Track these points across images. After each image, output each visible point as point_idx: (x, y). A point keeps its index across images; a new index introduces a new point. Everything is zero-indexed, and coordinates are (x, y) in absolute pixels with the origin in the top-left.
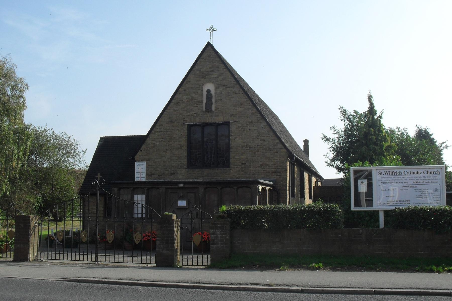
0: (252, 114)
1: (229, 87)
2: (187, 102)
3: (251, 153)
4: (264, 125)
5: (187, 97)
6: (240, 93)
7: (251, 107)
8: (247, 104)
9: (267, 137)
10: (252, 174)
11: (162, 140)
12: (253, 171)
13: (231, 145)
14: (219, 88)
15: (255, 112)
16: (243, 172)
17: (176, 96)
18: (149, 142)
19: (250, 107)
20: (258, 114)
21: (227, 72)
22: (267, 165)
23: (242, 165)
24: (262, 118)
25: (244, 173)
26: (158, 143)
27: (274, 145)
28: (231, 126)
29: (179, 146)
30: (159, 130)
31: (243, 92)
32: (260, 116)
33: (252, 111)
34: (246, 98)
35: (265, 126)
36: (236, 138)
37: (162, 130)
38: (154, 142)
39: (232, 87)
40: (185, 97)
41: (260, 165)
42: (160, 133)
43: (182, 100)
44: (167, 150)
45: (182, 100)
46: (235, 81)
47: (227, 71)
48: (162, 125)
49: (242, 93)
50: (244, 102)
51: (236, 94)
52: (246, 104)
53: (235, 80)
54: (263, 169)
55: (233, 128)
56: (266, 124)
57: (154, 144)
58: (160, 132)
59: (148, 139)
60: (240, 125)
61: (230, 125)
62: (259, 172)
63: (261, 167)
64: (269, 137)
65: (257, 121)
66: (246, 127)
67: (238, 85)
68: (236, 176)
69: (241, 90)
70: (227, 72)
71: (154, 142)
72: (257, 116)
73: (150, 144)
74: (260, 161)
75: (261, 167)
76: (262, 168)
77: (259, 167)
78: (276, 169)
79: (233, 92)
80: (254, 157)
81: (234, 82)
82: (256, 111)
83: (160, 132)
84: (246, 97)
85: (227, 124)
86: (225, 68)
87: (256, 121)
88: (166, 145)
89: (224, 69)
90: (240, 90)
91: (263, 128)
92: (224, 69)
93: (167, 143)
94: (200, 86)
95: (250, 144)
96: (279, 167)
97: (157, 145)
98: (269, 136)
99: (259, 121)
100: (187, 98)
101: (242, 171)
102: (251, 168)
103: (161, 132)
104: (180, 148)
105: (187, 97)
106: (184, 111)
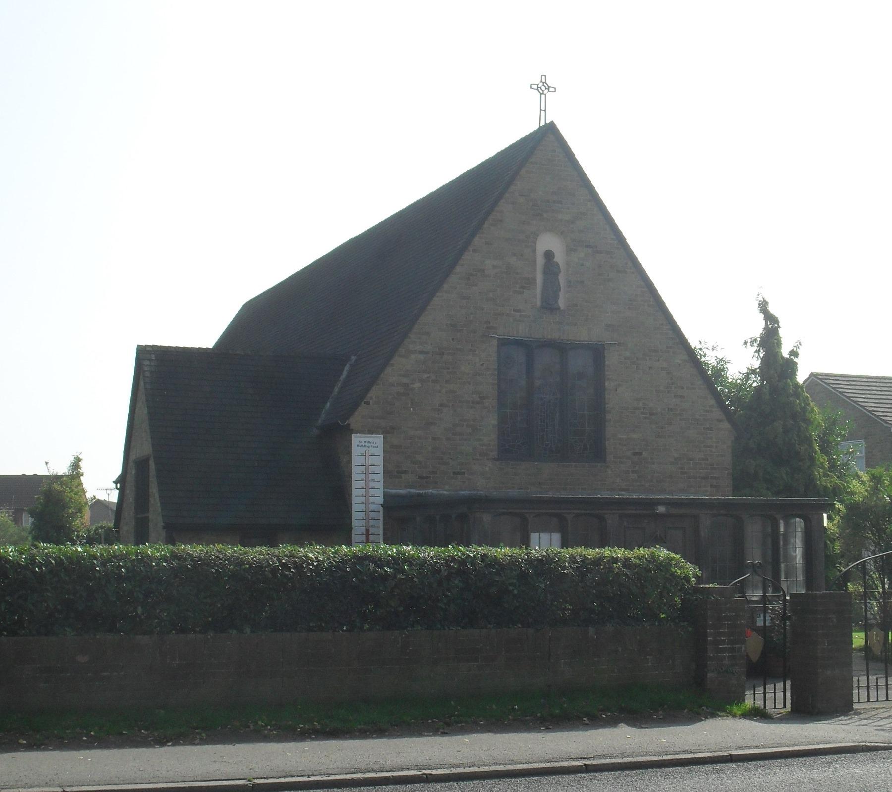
11: (428, 375)
13: (607, 404)
26: (417, 385)
38: (405, 380)
42: (422, 357)
43: (483, 271)
45: (483, 271)
46: (614, 237)
49: (633, 273)
51: (618, 271)
56: (686, 357)
58: (421, 352)
60: (628, 354)
65: (667, 347)
73: (393, 385)
83: (421, 352)
96: (715, 466)
100: (494, 267)
101: (633, 472)
103: (427, 353)
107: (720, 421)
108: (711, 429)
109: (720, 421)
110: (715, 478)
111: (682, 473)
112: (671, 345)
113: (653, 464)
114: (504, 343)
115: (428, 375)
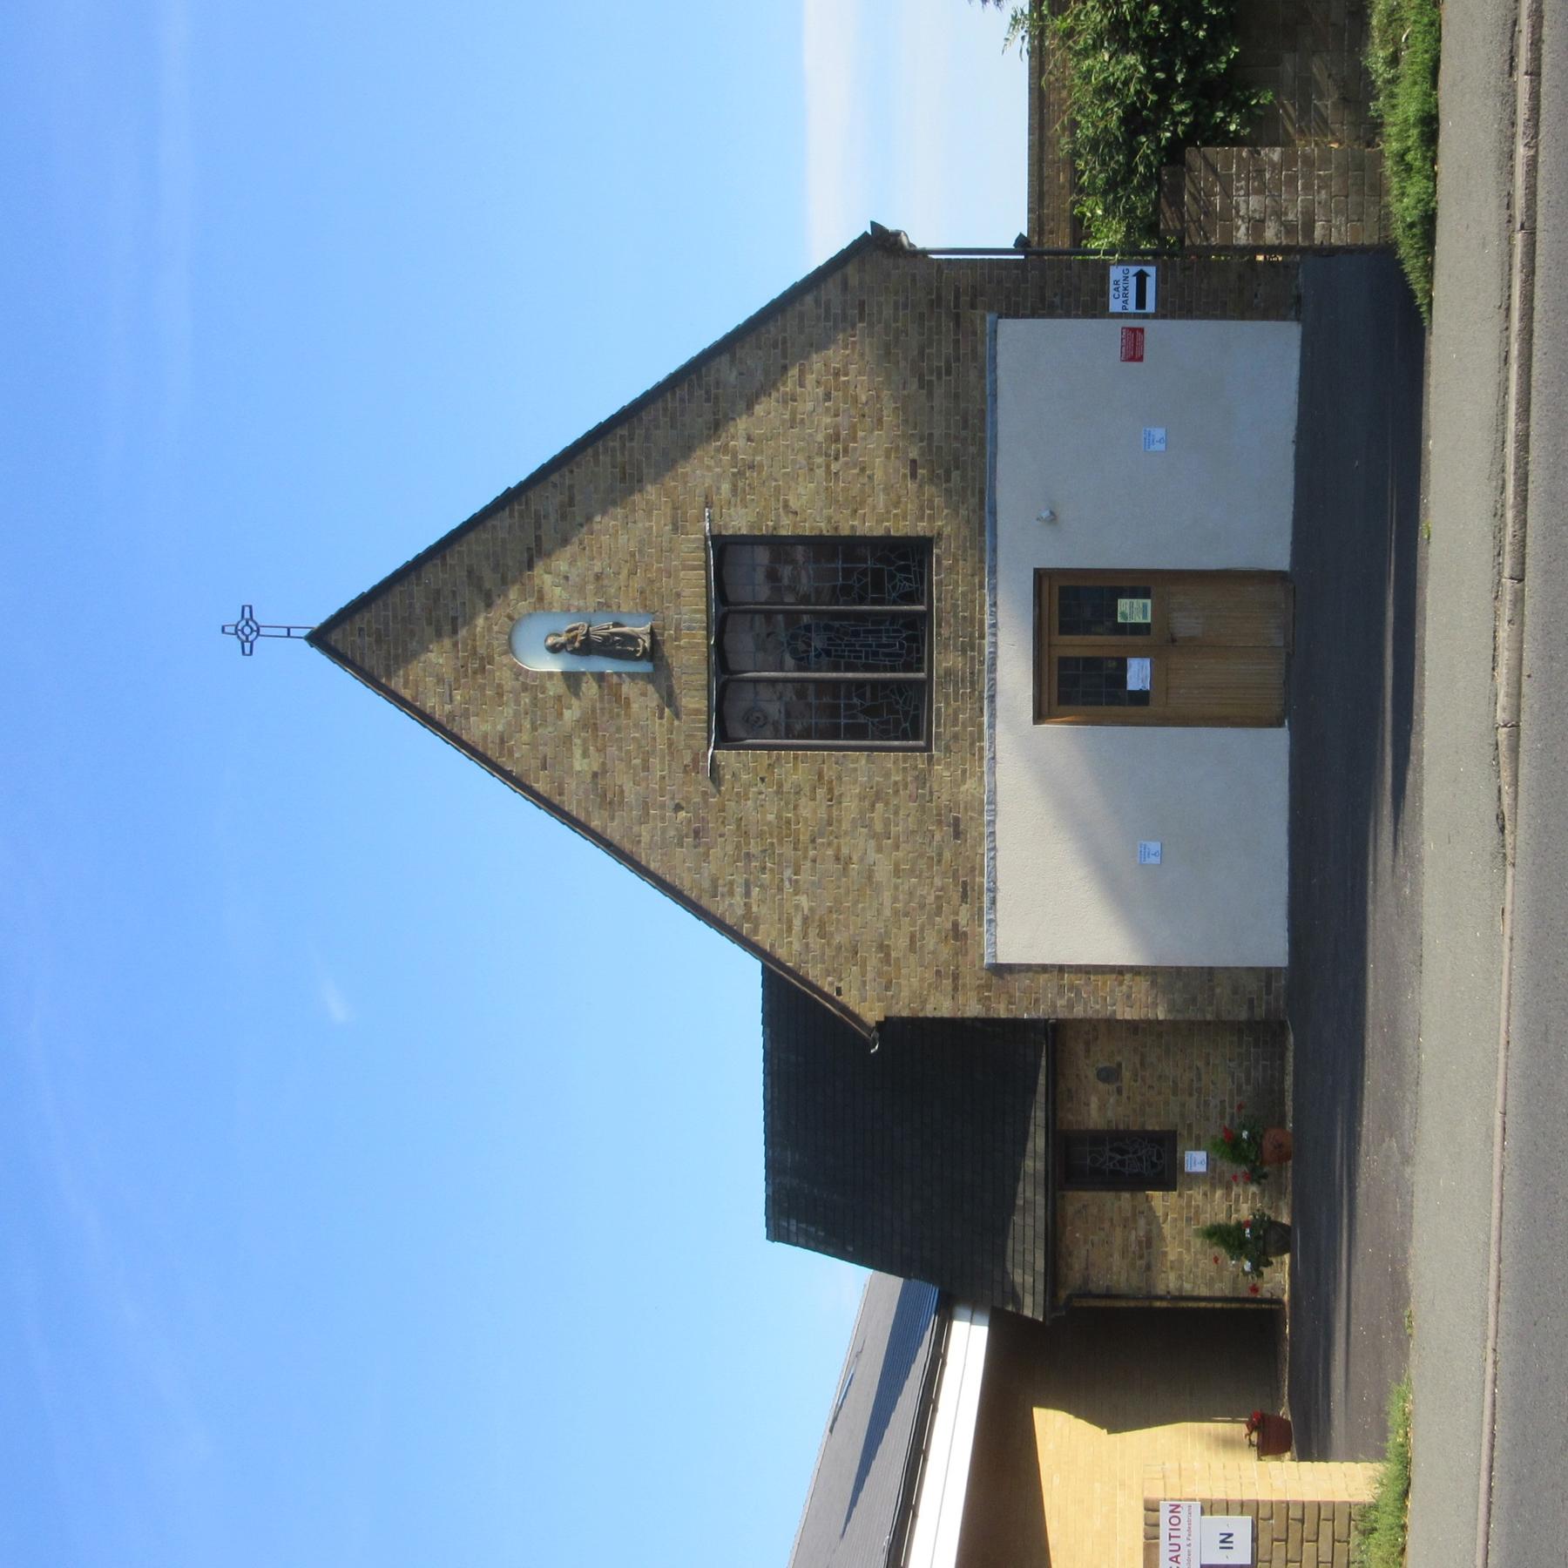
0: (671, 427)
1: (538, 539)
2: (601, 750)
3: (861, 434)
4: (730, 369)
5: (578, 752)
6: (567, 482)
7: (637, 431)
8: (623, 447)
9: (789, 351)
10: (965, 427)
11: (787, 883)
12: (948, 427)
13: (822, 531)
14: (540, 591)
15: (665, 410)
16: (955, 475)
17: (572, 808)
18: (796, 946)
19: (640, 432)
20: (674, 394)
21: (464, 548)
22: (921, 353)
23: (919, 477)
24: (694, 377)
25: (957, 468)
27: (827, 319)
28: (730, 532)
29: (821, 792)
30: (738, 899)
31: (565, 470)
32: (686, 386)
33: (657, 427)
34: (596, 455)
35: (733, 361)
36: (786, 505)
37: (739, 879)
38: (797, 922)
39: (538, 526)
40: (579, 764)
41: (921, 387)
42: (756, 891)
43: (595, 775)
44: (838, 859)
45: (595, 775)
46: (507, 510)
47: (457, 548)
48: (714, 882)
49: (572, 472)
50: (614, 467)
51: (571, 503)
52: (623, 454)
53: (503, 509)
54: (939, 378)
55: (739, 522)
56: (725, 358)
57: (805, 920)
58: (748, 894)
59: (781, 953)
60: (726, 487)
61: (724, 533)
62: (957, 396)
63: (930, 382)
64: (789, 345)
65: (708, 400)
66: (735, 456)
67: (531, 494)
68: (974, 511)
69: (555, 478)
70: (460, 548)
71: (797, 922)
72: (682, 400)
73: (807, 945)
74: (901, 386)
75: (930, 382)
76: (934, 378)
77: (930, 395)
78: (943, 315)
79: (563, 517)
80: (880, 421)
81: (512, 511)
82: (660, 404)
83: (748, 894)
84: (590, 451)
85: (723, 548)
86: (444, 558)
87: (709, 404)
88: (814, 861)
89: (449, 561)
90: (555, 485)
91: (741, 374)
92: (444, 564)
93: (805, 858)
94: (525, 688)
95: (820, 438)
96: (934, 297)
97: (811, 909)
98: (784, 341)
99: (708, 392)
100: (585, 754)
101: (948, 480)
102: (936, 433)
103: (747, 885)
104: (831, 790)
105: (578, 752)
106: (646, 768)
107: (845, 286)
108: (862, 304)
109: (845, 286)
110: (957, 298)
111: (948, 373)
112: (703, 392)
113: (931, 435)
114: (724, 738)
115: (787, 883)
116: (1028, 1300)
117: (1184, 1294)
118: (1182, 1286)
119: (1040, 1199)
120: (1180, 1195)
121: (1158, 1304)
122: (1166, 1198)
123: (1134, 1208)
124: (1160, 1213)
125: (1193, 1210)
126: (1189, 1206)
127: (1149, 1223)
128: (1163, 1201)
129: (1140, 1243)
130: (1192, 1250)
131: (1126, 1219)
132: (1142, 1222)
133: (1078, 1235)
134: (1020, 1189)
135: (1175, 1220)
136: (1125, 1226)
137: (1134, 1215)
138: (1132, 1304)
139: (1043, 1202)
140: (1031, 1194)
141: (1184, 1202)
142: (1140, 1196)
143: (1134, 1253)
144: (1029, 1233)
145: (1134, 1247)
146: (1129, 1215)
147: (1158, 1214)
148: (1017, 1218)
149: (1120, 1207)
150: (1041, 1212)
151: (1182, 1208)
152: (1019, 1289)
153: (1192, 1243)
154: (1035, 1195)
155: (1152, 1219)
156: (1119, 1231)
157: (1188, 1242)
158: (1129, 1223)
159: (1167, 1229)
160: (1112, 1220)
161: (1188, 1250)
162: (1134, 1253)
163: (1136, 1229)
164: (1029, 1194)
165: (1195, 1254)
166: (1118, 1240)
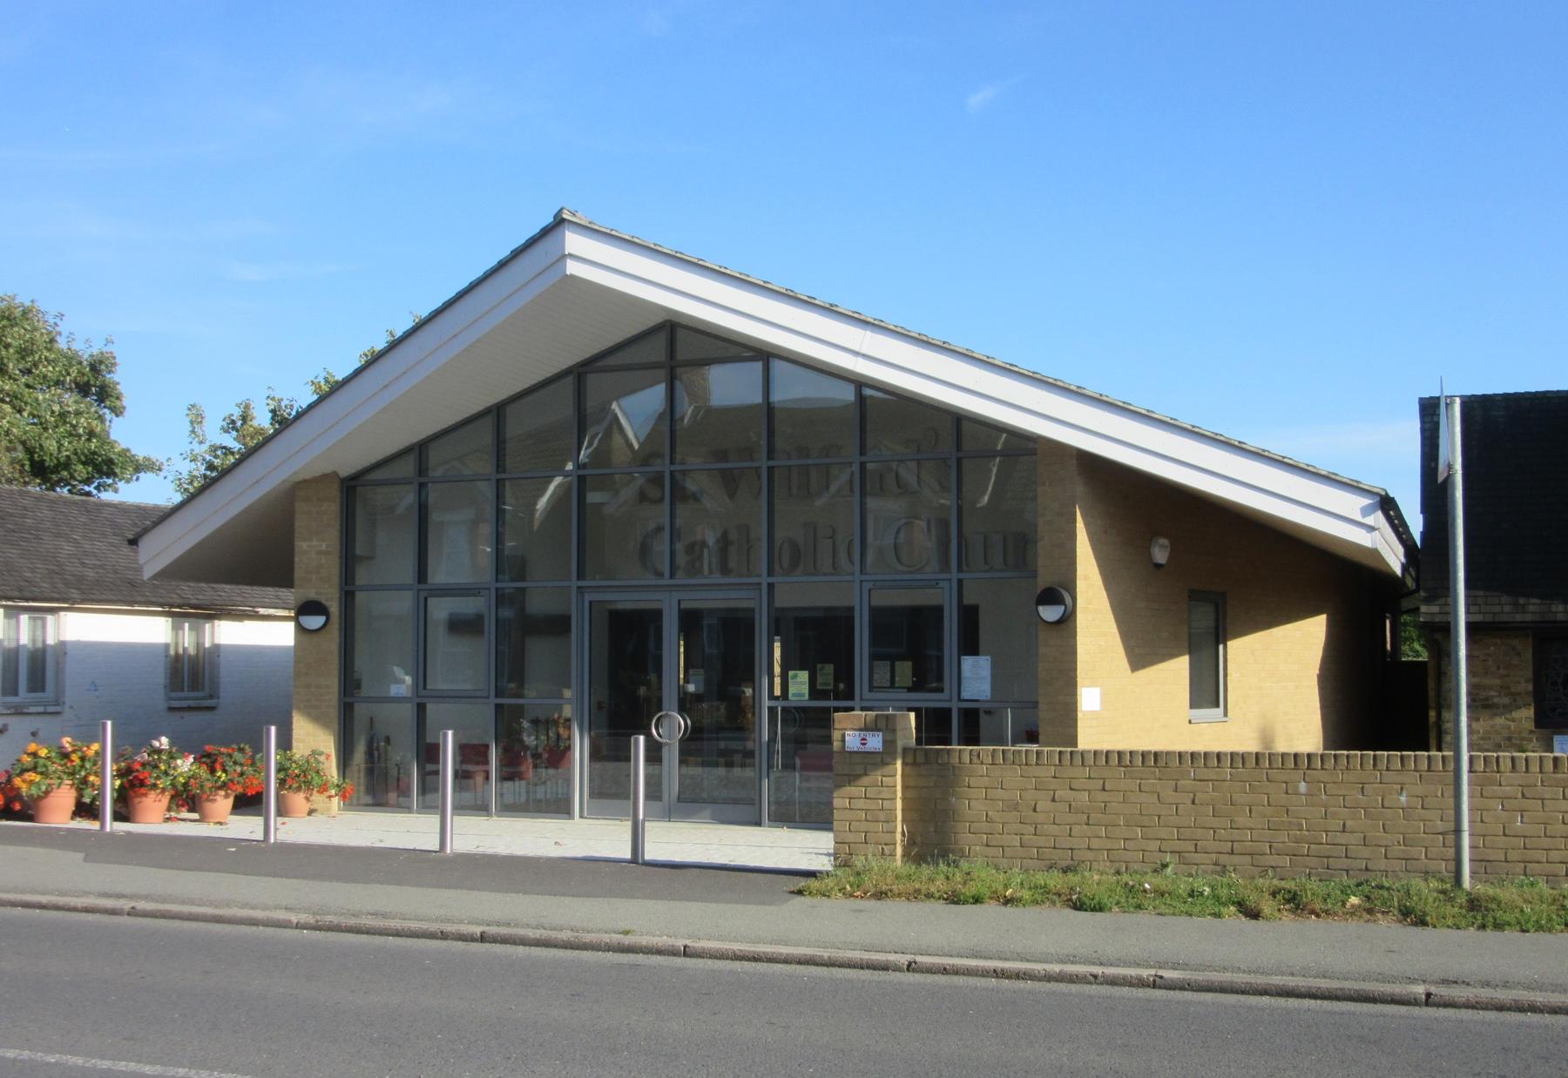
116: (1435, 609)
117: (1443, 735)
118: (1448, 733)
119: (1528, 617)
120: (1531, 732)
121: (1432, 714)
122: (1529, 720)
123: (1519, 694)
124: (1516, 714)
125: (1518, 742)
126: (1523, 739)
127: (1505, 706)
128: (1526, 718)
129: (1487, 699)
130: (1482, 742)
131: (1508, 688)
132: (1506, 700)
133: (1492, 648)
134: (1534, 601)
135: (1509, 728)
136: (1501, 687)
137: (1512, 694)
138: (1432, 694)
139: (1527, 620)
140: (1533, 609)
141: (1525, 735)
142: (1530, 699)
143: (1478, 694)
144: (1497, 609)
145: (1483, 694)
146: (1512, 690)
147: (1513, 713)
148: (1504, 599)
149: (1519, 682)
150: (1518, 618)
151: (1520, 733)
152: (1442, 601)
153: (1487, 742)
154: (1531, 613)
155: (1508, 709)
156: (1497, 682)
157: (1490, 738)
158: (1505, 689)
159: (1500, 721)
160: (1508, 676)
161: (1482, 739)
162: (1478, 694)
163: (1500, 696)
164: (1531, 608)
165: (1477, 745)
166: (1488, 681)
